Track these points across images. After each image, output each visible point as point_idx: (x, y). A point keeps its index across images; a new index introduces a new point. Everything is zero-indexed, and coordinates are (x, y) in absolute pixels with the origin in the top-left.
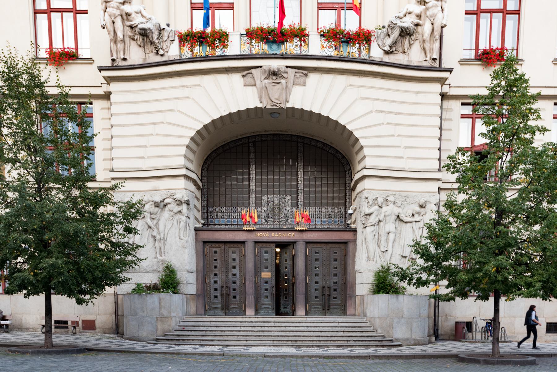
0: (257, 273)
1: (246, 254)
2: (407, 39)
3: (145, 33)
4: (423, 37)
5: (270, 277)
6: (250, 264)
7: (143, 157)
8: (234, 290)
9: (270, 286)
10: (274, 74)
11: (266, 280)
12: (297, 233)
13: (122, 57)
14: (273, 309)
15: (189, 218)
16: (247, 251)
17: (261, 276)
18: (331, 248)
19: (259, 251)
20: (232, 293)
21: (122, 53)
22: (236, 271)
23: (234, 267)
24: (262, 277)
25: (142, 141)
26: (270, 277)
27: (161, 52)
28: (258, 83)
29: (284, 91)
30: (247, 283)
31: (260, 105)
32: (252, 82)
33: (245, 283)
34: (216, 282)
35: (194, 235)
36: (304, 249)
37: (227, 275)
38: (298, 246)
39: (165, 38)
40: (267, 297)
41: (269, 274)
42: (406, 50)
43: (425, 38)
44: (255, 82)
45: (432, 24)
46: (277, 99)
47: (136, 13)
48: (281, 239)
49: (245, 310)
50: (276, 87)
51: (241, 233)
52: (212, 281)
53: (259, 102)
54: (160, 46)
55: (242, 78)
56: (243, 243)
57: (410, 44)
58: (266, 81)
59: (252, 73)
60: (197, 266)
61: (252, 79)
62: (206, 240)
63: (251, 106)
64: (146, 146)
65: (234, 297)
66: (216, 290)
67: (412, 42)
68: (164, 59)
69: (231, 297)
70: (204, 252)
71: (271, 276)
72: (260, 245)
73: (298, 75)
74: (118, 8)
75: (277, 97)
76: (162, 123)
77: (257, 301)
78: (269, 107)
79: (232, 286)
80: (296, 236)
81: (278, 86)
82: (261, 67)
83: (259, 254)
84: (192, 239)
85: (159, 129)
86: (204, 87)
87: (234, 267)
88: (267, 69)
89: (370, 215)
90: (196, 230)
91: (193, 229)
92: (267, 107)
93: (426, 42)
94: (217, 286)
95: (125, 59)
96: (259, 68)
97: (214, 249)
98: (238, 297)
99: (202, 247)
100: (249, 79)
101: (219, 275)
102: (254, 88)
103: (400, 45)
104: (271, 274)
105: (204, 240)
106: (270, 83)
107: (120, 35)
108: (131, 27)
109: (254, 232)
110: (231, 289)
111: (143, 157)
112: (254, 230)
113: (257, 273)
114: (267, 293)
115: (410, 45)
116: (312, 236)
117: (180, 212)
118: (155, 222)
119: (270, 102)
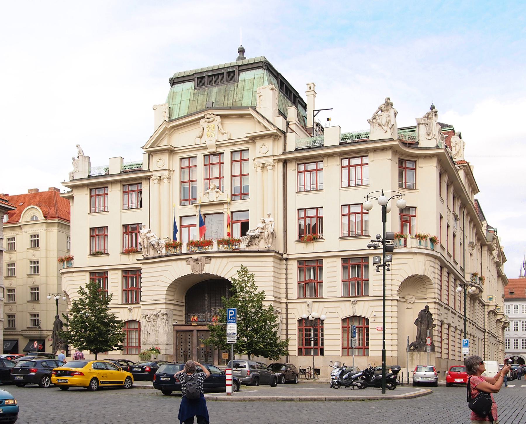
3: (153, 245)
6: (195, 341)
7: (152, 295)
8: (189, 353)
10: (196, 260)
13: (147, 254)
20: (189, 354)
21: (147, 252)
22: (190, 344)
23: (189, 342)
25: (151, 288)
27: (159, 252)
28: (191, 264)
29: (200, 267)
31: (192, 273)
34: (182, 349)
37: (186, 346)
39: (161, 247)
40: (203, 356)
47: (152, 236)
52: (180, 349)
54: (158, 250)
56: (193, 331)
58: (193, 263)
63: (189, 273)
65: (189, 356)
66: (182, 352)
68: (160, 255)
73: (206, 259)
74: (145, 235)
78: (195, 273)
79: (189, 351)
81: (198, 265)
87: (189, 342)
95: (147, 255)
101: (183, 346)
107: (146, 246)
108: (150, 243)
111: (152, 295)
112: (196, 325)
114: (203, 354)
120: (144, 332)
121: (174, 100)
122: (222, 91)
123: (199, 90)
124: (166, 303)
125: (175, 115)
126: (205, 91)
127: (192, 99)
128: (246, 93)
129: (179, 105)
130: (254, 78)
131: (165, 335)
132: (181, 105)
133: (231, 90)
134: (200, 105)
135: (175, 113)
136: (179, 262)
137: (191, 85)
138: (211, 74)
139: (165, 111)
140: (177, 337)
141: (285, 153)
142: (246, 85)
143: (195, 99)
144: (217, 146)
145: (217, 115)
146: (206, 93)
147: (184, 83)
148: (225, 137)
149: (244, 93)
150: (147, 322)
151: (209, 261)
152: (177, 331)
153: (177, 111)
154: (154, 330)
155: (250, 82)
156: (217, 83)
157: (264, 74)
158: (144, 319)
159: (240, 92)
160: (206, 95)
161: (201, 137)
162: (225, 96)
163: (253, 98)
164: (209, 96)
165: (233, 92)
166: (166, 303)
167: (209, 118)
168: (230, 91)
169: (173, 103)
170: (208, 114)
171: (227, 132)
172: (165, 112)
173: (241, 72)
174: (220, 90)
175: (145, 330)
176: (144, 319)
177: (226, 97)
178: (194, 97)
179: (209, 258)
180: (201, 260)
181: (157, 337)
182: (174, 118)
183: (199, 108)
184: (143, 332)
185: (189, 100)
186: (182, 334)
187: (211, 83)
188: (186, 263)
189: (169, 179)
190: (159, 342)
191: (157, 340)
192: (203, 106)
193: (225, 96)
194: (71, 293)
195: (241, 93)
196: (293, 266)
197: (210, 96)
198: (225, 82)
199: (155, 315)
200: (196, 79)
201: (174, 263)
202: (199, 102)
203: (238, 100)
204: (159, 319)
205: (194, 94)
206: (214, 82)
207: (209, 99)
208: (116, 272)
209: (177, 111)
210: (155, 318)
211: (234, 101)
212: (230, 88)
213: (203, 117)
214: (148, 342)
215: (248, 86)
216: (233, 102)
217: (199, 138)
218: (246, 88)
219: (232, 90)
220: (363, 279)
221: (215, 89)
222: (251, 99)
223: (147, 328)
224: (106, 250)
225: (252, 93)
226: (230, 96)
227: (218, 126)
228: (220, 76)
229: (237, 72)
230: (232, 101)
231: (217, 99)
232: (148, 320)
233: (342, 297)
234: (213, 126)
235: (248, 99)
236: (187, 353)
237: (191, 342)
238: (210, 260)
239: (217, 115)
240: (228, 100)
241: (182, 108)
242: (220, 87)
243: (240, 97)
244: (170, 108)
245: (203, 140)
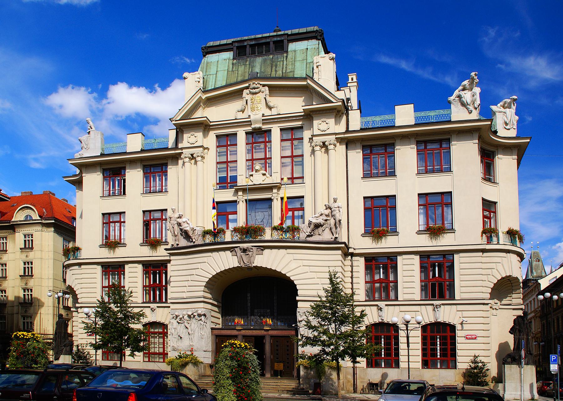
31: (240, 265)
59: (235, 250)
82: (239, 247)
89: (301, 321)
100: (234, 252)
117: (201, 320)
118: (189, 325)
121: (208, 70)
122: (269, 62)
123: (239, 60)
125: (210, 86)
126: (246, 61)
127: (231, 70)
128: (298, 64)
129: (215, 76)
130: (307, 49)
132: (217, 76)
133: (279, 60)
134: (241, 76)
135: (211, 83)
136: (222, 253)
137: (228, 55)
138: (253, 43)
139: (198, 80)
141: (348, 131)
142: (298, 56)
143: (234, 70)
144: (266, 121)
145: (264, 86)
146: (248, 63)
147: (220, 53)
148: (274, 111)
149: (295, 64)
153: (212, 82)
155: (302, 53)
156: (260, 54)
157: (319, 44)
159: (290, 63)
160: (248, 66)
161: (243, 111)
162: (272, 67)
163: (307, 69)
164: (252, 66)
165: (282, 63)
167: (255, 89)
168: (278, 61)
169: (207, 74)
170: (253, 84)
171: (276, 106)
172: (199, 82)
173: (291, 42)
174: (265, 61)
177: (274, 68)
178: (233, 67)
182: (210, 88)
183: (240, 79)
185: (226, 72)
187: (253, 53)
189: (203, 157)
192: (244, 77)
193: (272, 67)
194: (79, 289)
195: (292, 64)
196: (360, 263)
197: (253, 67)
198: (271, 52)
200: (235, 48)
201: (215, 254)
202: (240, 72)
203: (288, 71)
205: (233, 64)
206: (257, 52)
207: (252, 69)
208: (136, 265)
209: (212, 82)
211: (284, 72)
212: (278, 58)
213: (247, 88)
215: (299, 57)
216: (282, 73)
217: (241, 111)
218: (298, 59)
219: (280, 61)
220: (446, 279)
221: (259, 60)
222: (305, 70)
224: (122, 240)
225: (305, 64)
226: (278, 67)
227: (265, 98)
228: (264, 46)
229: (286, 41)
230: (281, 72)
231: (262, 70)
233: (421, 300)
234: (258, 98)
235: (301, 71)
238: (263, 250)
239: (264, 86)
240: (276, 71)
241: (218, 79)
242: (265, 57)
243: (291, 68)
244: (204, 78)
245: (245, 115)
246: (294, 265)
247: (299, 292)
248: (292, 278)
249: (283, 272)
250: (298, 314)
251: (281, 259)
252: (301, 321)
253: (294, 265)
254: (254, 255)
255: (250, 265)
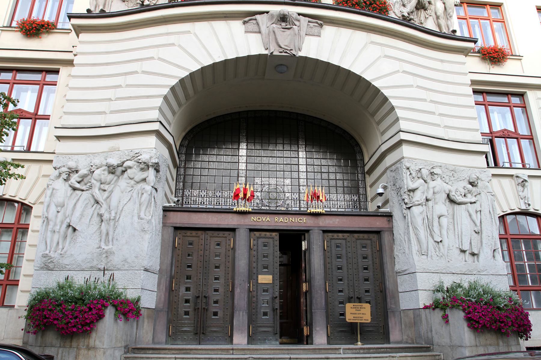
0: (252, 276)
1: (237, 247)
2: (422, 12)
4: (436, 14)
5: (271, 282)
8: (216, 302)
9: (271, 296)
11: (265, 287)
12: (310, 217)
14: (277, 333)
15: (156, 190)
16: (237, 242)
17: (257, 280)
18: (357, 239)
19: (255, 242)
20: (213, 308)
24: (259, 282)
26: (271, 282)
28: (263, 29)
30: (237, 291)
32: (256, 29)
33: (233, 292)
34: (188, 289)
35: (161, 217)
36: (321, 240)
38: (312, 236)
40: (265, 314)
41: (270, 277)
42: (422, 21)
43: (438, 14)
44: (259, 29)
45: (444, 3)
46: (286, 46)
48: (287, 226)
49: (231, 337)
50: (285, 33)
51: (230, 216)
52: (183, 290)
53: (263, 49)
55: (244, 26)
56: (233, 230)
57: (425, 18)
58: (274, 25)
59: (256, 20)
60: (161, 264)
61: (256, 26)
62: (178, 225)
64: (110, 100)
66: (187, 301)
67: (427, 16)
69: (210, 314)
70: (174, 242)
71: (273, 280)
72: (257, 234)
75: (287, 44)
76: (136, 72)
77: (251, 321)
78: (276, 53)
79: (215, 296)
80: (308, 221)
82: (267, 12)
83: (255, 247)
84: (157, 221)
85: (130, 80)
86: (195, 35)
88: (275, 14)
90: (166, 210)
91: (161, 208)
92: (274, 54)
93: (440, 18)
94: (190, 295)
96: (266, 14)
97: (191, 239)
98: (220, 314)
99: (172, 235)
100: (251, 26)
102: (259, 35)
103: (416, 16)
104: (273, 277)
105: (175, 225)
106: (279, 28)
109: (249, 216)
110: (212, 302)
113: (252, 276)
115: (426, 18)
116: (331, 222)
119: (278, 48)
120: (55, 225)
124: (157, 133)
131: (147, 236)
136: (220, 25)
140: (174, 247)
150: (70, 190)
151: (316, 30)
152: (176, 229)
154: (96, 219)
158: (61, 180)
166: (157, 133)
175: (59, 220)
176: (61, 180)
179: (319, 22)
180: (297, 23)
181: (107, 242)
184: (51, 224)
186: (191, 239)
188: (243, 27)
190: (116, 260)
191: (108, 254)
199: (112, 170)
204: (123, 182)
210: (111, 176)
214: (66, 261)
223: (69, 212)
232: (77, 186)
236: (207, 304)
237: (222, 267)
238: (321, 26)
246: (387, 66)
247: (403, 125)
248: (386, 92)
249: (367, 76)
250: (405, 174)
251: (360, 52)
252: (413, 191)
253: (387, 66)
254: (303, 33)
255: (294, 52)
